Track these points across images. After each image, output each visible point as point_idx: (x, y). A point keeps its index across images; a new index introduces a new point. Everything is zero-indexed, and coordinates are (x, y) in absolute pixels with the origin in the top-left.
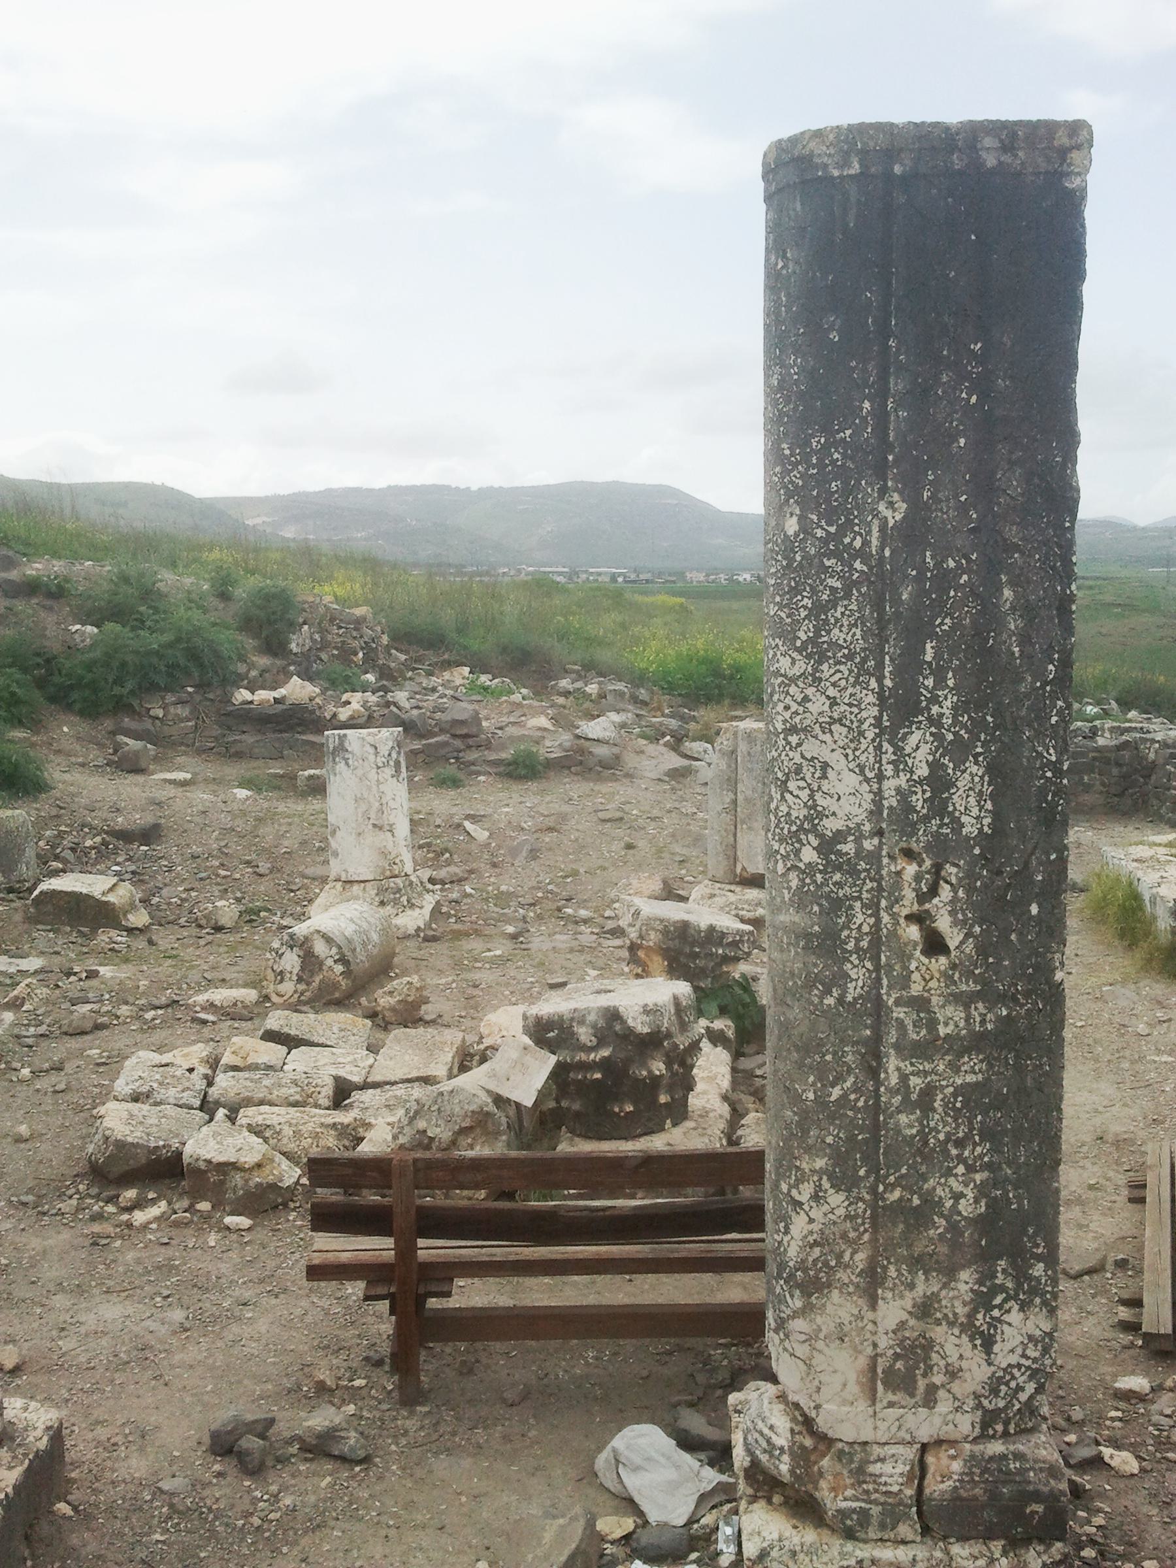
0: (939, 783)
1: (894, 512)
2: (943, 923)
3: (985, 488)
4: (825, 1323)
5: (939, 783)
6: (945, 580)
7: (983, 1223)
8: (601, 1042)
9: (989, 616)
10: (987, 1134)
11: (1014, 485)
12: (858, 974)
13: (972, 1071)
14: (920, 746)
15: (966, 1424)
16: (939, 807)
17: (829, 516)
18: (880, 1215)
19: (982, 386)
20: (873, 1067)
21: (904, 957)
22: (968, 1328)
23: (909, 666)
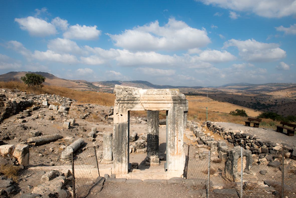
0: (154, 131)
1: (152, 120)
2: (154, 136)
3: (155, 119)
4: (149, 153)
5: (154, 131)
6: (154, 123)
7: (156, 149)
8: (140, 143)
9: (156, 124)
10: (156, 145)
11: (156, 119)
12: (150, 138)
13: (155, 142)
14: (153, 129)
15: (155, 158)
16: (154, 132)
17: (149, 120)
18: (151, 149)
19: (155, 115)
20: (151, 142)
21: (152, 138)
22: (155, 153)
23: (152, 126)
